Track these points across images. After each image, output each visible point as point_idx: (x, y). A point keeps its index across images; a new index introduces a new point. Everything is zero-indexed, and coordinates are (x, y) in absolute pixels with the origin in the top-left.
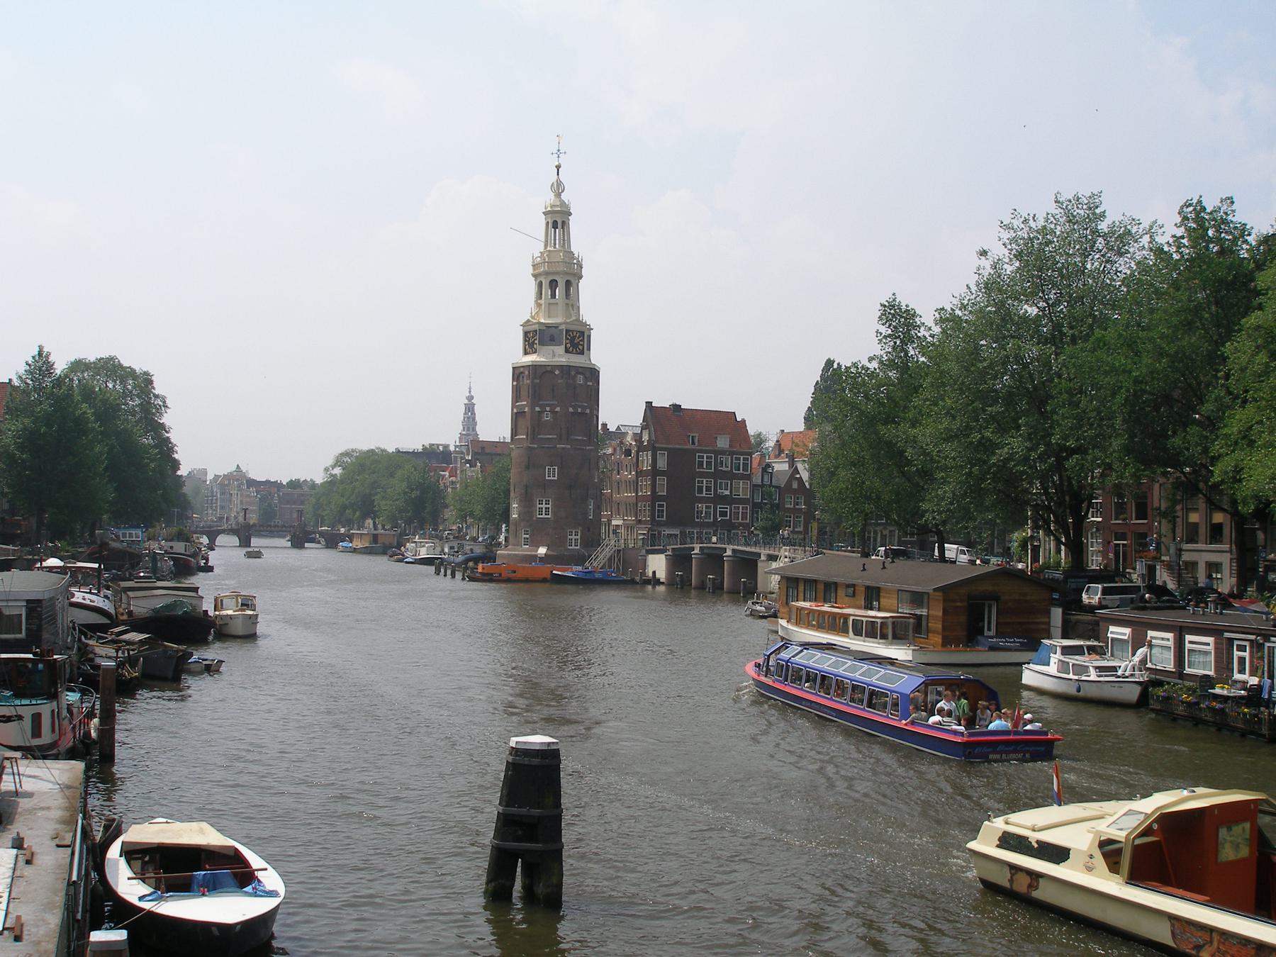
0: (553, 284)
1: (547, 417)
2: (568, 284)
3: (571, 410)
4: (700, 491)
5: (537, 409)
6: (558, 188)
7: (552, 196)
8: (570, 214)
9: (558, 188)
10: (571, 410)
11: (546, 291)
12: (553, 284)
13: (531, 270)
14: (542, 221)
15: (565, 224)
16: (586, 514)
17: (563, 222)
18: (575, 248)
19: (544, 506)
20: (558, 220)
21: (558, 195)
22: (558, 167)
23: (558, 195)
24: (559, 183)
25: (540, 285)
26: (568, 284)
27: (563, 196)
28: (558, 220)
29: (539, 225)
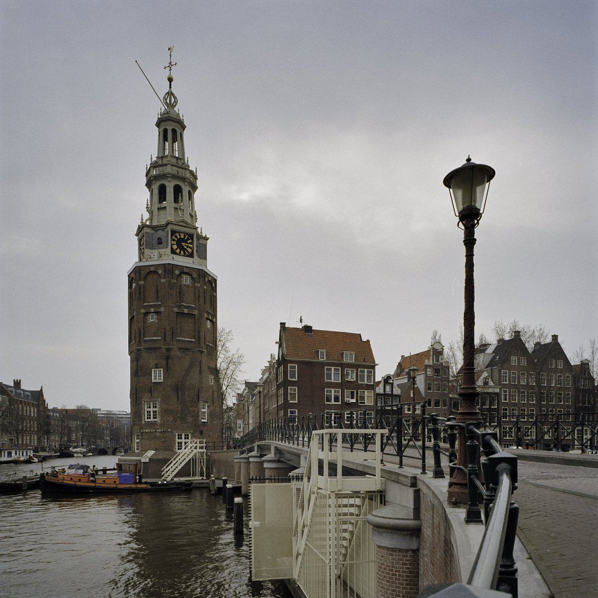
1: (152, 319)
2: (178, 190)
3: (176, 310)
4: (329, 400)
5: (143, 311)
10: (176, 310)
12: (162, 191)
14: (155, 132)
16: (196, 416)
17: (174, 131)
19: (152, 409)
20: (171, 128)
23: (172, 106)
24: (170, 94)
26: (178, 190)
28: (171, 128)
29: (154, 133)
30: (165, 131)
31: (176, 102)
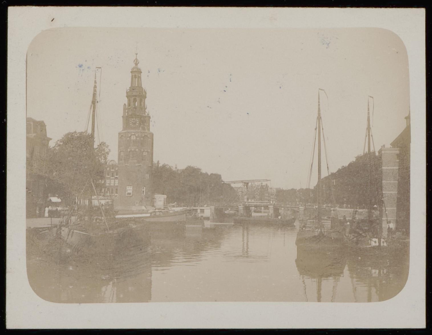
0: (135, 101)
2: (141, 101)
6: (136, 62)
7: (134, 65)
8: (141, 72)
9: (136, 62)
11: (132, 104)
13: (125, 94)
14: (130, 75)
15: (140, 78)
18: (143, 86)
21: (136, 64)
22: (137, 54)
23: (136, 64)
24: (136, 59)
25: (129, 101)
27: (139, 66)
28: (136, 73)
30: (135, 76)
31: (138, 63)
